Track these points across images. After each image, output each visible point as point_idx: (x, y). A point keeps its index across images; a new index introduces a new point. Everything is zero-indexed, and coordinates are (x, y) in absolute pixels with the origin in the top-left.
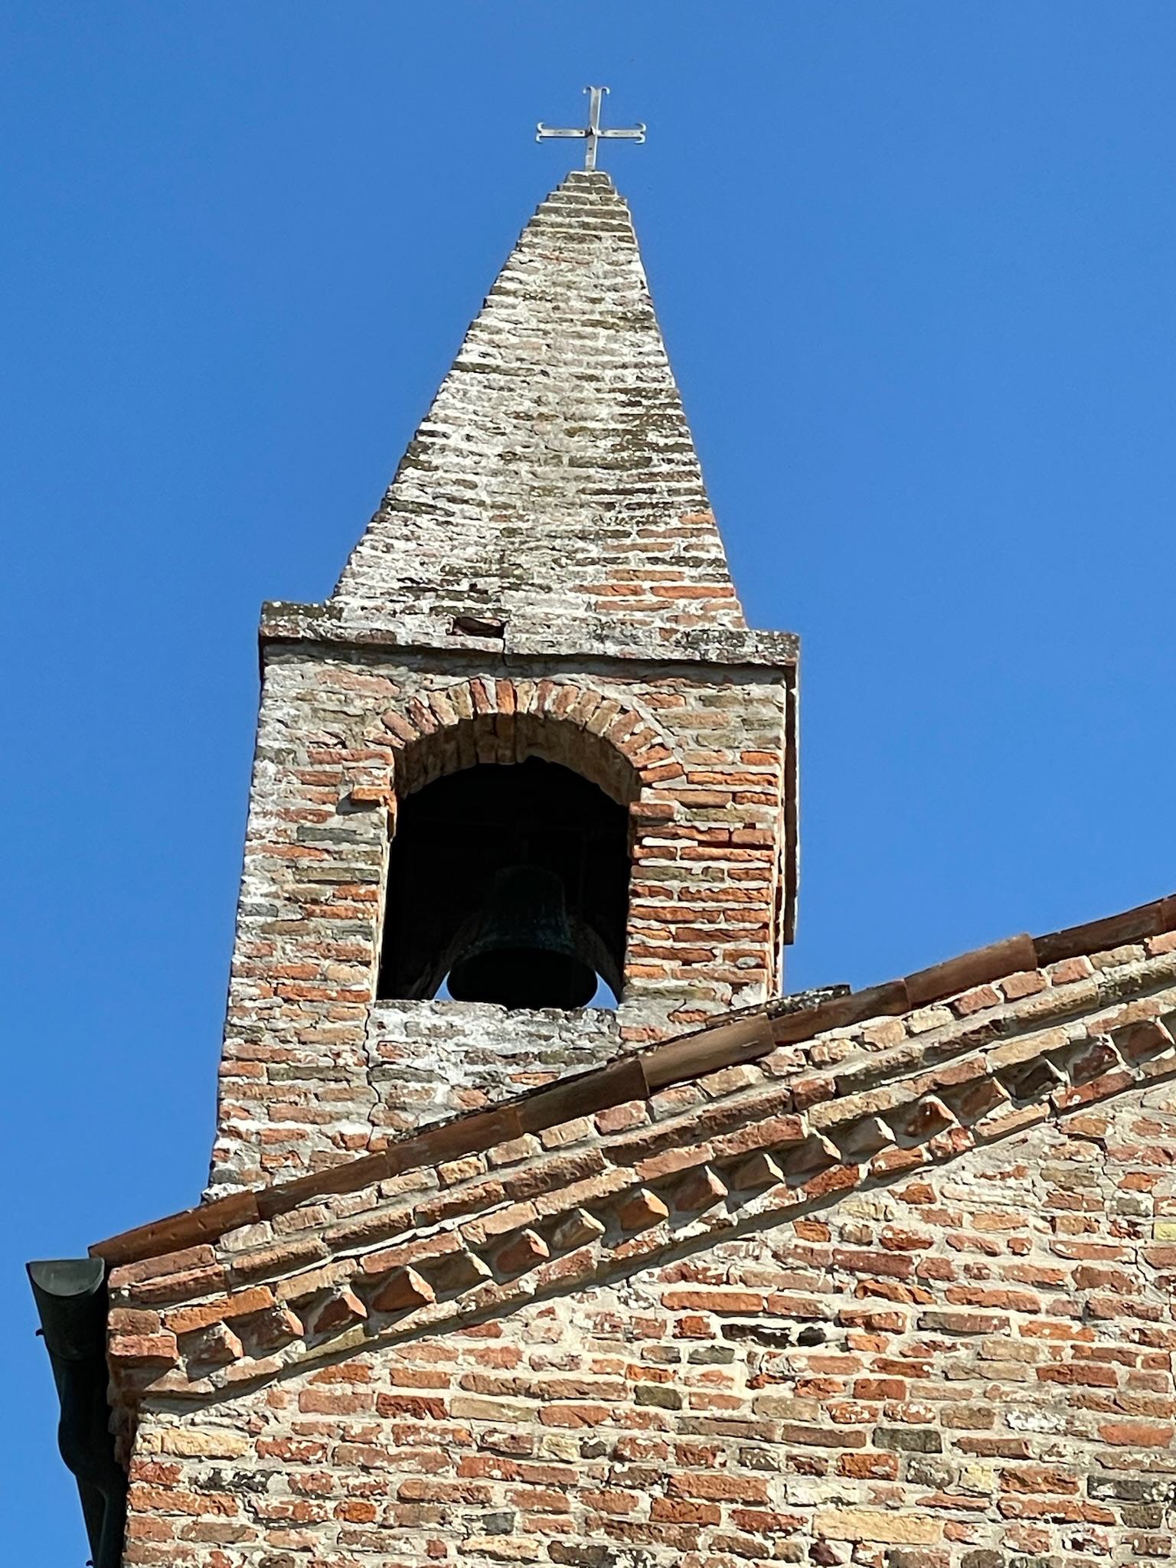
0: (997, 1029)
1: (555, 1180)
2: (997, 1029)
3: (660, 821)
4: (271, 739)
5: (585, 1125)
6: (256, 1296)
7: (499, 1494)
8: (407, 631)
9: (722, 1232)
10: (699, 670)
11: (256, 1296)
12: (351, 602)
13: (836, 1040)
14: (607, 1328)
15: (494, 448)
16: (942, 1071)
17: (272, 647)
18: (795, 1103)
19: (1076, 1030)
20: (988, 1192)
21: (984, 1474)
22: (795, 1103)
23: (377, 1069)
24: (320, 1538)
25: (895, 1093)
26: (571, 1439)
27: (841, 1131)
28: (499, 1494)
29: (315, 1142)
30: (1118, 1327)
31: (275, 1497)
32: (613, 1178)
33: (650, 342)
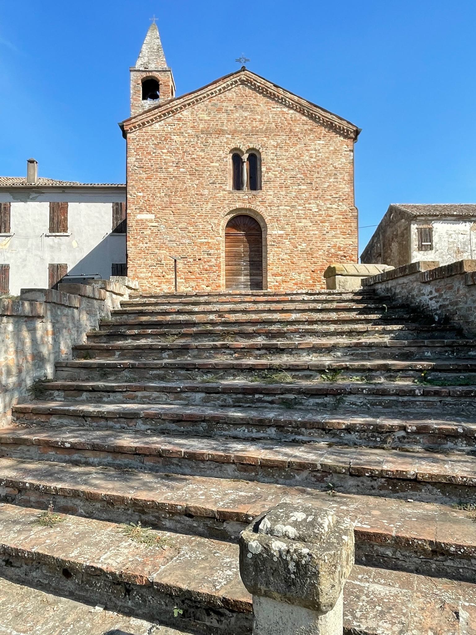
0: (186, 101)
1: (155, 114)
2: (186, 101)
3: (161, 84)
4: (131, 79)
5: (157, 110)
6: (134, 125)
7: (153, 138)
8: (141, 69)
9: (167, 118)
10: (163, 71)
11: (134, 125)
12: (136, 66)
13: (175, 102)
14: (160, 126)
15: (147, 51)
16: (182, 104)
17: (131, 71)
18: (172, 107)
19: (192, 100)
20: (187, 113)
21: (186, 135)
22: (172, 107)
23: (142, 106)
24: (141, 143)
25: (179, 106)
26: (158, 134)
27: (176, 109)
28: (153, 138)
29: (138, 112)
30: (195, 124)
31: (137, 140)
32: (159, 114)
33: (159, 40)
